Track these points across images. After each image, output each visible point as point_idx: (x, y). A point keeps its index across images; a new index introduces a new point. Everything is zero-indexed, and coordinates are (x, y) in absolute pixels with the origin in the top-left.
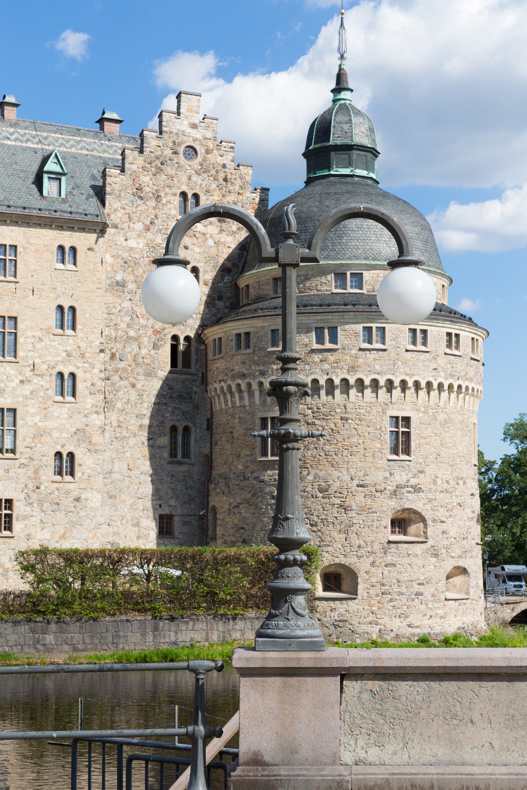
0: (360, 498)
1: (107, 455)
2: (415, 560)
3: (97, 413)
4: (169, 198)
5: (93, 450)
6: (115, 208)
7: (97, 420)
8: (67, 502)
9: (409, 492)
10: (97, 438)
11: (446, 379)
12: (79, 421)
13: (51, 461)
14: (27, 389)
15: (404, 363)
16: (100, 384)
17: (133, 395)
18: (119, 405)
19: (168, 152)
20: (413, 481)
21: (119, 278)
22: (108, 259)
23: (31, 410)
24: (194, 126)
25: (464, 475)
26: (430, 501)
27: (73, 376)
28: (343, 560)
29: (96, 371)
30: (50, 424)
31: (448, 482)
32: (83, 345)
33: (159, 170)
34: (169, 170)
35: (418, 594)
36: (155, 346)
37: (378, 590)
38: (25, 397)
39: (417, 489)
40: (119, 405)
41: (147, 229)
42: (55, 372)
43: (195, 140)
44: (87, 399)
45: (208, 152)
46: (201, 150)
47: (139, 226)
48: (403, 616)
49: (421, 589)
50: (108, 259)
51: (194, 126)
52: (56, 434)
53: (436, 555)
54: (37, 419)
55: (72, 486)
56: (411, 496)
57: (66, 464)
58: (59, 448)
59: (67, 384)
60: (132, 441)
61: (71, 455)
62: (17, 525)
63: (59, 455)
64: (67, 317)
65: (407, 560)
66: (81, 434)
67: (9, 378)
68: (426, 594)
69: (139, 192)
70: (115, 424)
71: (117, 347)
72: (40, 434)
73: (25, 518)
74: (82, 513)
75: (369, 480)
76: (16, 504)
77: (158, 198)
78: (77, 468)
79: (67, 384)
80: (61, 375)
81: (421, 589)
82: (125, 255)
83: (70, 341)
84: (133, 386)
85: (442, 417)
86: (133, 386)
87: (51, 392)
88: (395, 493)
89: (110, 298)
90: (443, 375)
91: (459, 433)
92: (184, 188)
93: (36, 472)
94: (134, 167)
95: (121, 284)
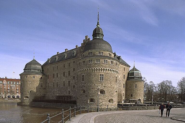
7: (77, 81)
10: (77, 83)
49: (84, 101)
57: (74, 87)
81: (84, 101)
85: (89, 74)
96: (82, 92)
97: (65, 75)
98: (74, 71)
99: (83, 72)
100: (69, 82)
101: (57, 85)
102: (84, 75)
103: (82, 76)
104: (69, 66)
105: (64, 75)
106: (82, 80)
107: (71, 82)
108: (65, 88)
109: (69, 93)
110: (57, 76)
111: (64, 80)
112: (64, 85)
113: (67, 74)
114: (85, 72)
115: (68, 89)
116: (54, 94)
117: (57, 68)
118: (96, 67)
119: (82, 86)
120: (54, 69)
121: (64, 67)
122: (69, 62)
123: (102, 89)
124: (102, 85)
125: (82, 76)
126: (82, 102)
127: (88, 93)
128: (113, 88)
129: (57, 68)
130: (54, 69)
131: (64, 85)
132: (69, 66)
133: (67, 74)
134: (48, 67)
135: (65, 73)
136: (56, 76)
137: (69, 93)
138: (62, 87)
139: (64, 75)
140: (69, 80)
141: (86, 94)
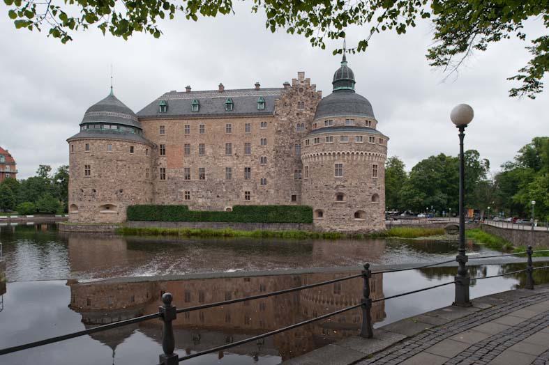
0: (325, 190)
1: (276, 179)
5: (272, 178)
7: (273, 170)
13: (260, 181)
14: (253, 162)
15: (339, 147)
16: (274, 160)
19: (294, 91)
24: (302, 82)
28: (321, 208)
33: (291, 97)
36: (290, 148)
37: (331, 217)
39: (344, 187)
46: (304, 89)
47: (285, 114)
51: (302, 82)
57: (264, 182)
62: (251, 199)
64: (264, 141)
67: (248, 160)
69: (285, 104)
71: (278, 149)
72: (257, 174)
77: (291, 105)
79: (263, 160)
80: (262, 158)
85: (355, 163)
93: (256, 184)
95: (280, 131)
97: (234, 152)
101: (202, 176)
105: (229, 151)
107: (254, 170)
109: (247, 197)
110: (202, 151)
111: (229, 162)
112: (229, 176)
113: (238, 148)
115: (242, 187)
116: (188, 197)
121: (229, 130)
122: (249, 121)
125: (334, 166)
131: (229, 176)
133: (238, 148)
135: (233, 146)
137: (247, 197)
138: (220, 181)
139: (229, 151)
140: (248, 166)
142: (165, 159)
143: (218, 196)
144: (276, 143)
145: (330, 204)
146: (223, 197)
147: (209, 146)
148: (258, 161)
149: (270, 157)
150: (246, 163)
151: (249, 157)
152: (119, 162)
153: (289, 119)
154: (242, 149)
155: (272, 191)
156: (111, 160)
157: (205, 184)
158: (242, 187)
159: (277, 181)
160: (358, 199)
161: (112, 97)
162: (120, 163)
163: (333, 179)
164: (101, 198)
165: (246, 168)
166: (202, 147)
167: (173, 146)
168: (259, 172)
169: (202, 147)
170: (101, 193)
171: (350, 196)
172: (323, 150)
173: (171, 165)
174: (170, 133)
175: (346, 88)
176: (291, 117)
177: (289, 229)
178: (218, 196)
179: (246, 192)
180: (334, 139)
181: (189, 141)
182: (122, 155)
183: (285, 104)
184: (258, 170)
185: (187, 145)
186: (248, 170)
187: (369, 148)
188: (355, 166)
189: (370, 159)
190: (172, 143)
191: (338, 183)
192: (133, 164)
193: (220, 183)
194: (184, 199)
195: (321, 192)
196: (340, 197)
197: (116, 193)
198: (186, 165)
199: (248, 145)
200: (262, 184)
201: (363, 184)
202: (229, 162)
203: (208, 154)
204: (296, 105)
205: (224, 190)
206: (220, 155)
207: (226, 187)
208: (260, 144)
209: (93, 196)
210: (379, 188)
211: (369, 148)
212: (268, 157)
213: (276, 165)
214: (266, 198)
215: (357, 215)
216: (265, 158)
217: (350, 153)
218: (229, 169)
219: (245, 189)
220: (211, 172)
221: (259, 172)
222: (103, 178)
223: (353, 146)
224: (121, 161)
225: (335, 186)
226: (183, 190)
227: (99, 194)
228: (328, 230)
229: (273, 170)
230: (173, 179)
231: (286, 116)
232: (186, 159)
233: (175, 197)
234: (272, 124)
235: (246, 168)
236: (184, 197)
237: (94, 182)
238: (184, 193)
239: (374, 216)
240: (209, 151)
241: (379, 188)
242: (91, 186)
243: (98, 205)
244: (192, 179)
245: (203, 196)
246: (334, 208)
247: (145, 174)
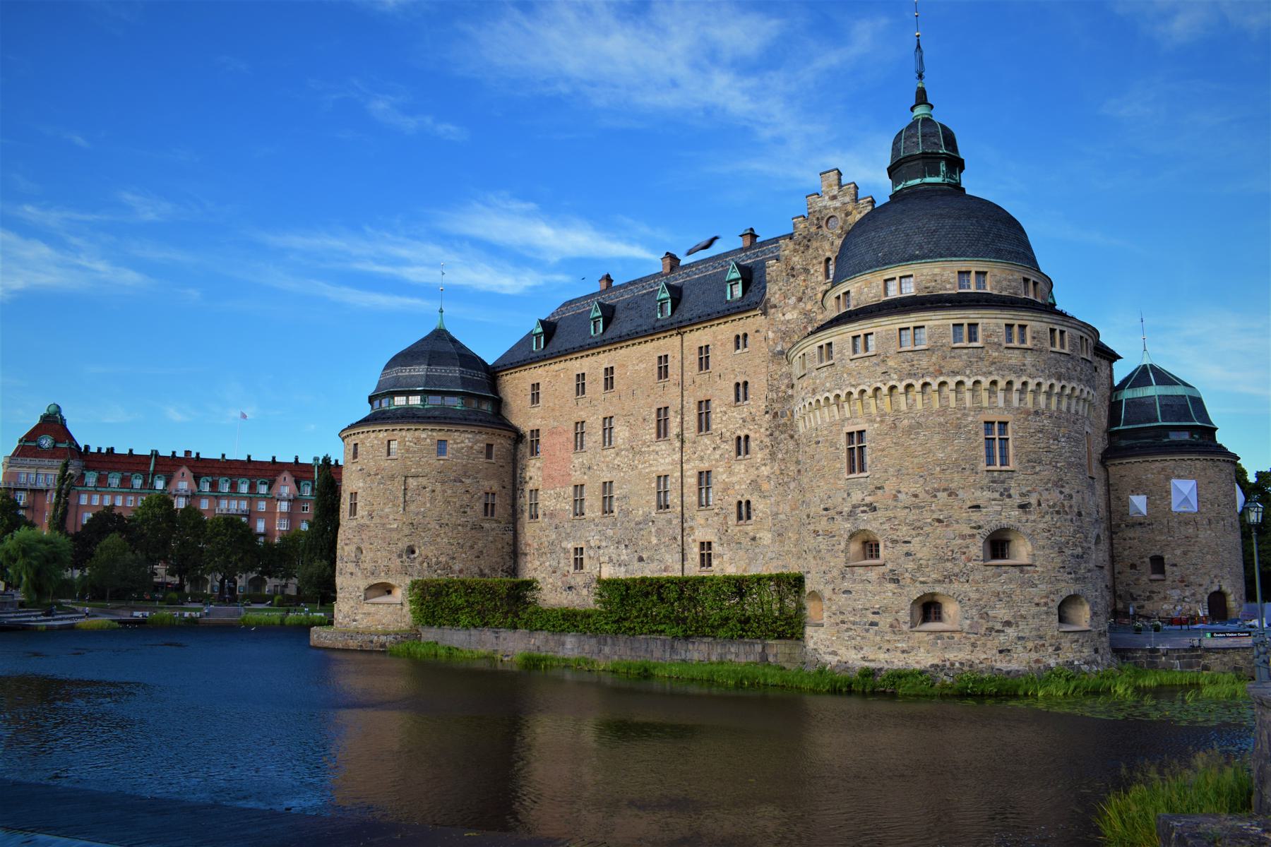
1: (773, 499)
2: (870, 587)
3: (765, 465)
4: (817, 267)
6: (774, 292)
7: (765, 471)
8: (746, 542)
9: (864, 512)
10: (765, 487)
11: (901, 380)
12: (753, 472)
13: (735, 510)
14: (718, 452)
16: (767, 441)
17: (791, 444)
18: (780, 456)
19: (813, 229)
20: (868, 500)
21: (779, 348)
22: (771, 335)
23: (721, 470)
25: (953, 486)
26: (889, 519)
27: (747, 437)
29: (762, 430)
30: (734, 479)
31: (916, 496)
32: (753, 411)
34: (814, 244)
35: (873, 624)
38: (717, 461)
40: (780, 456)
41: (800, 300)
42: (734, 437)
43: (835, 209)
44: (758, 455)
45: (848, 214)
47: (793, 300)
48: (858, 648)
49: (876, 618)
50: (771, 335)
51: (834, 198)
52: (737, 487)
53: (896, 581)
54: (724, 477)
55: (750, 528)
56: (865, 516)
57: (744, 511)
58: (739, 498)
59: (742, 445)
60: (792, 485)
61: (748, 502)
62: (715, 562)
63: (740, 503)
64: (742, 391)
65: (859, 587)
66: (755, 484)
68: (881, 624)
70: (778, 472)
71: (777, 406)
73: (721, 556)
74: (757, 550)
75: (829, 504)
76: (714, 545)
77: (806, 271)
78: (753, 513)
80: (739, 438)
81: (876, 618)
82: (783, 328)
83: (745, 409)
84: (792, 437)
86: (792, 437)
87: (733, 454)
88: (852, 514)
89: (772, 367)
90: (895, 377)
91: (936, 438)
92: (828, 254)
94: (787, 252)
96: (855, 547)
98: (737, 399)
99: (860, 412)
100: (704, 478)
102: (861, 433)
103: (850, 434)
104: (704, 363)
106: (845, 465)
107: (720, 477)
108: (670, 522)
109: (706, 560)
114: (873, 410)
116: (579, 564)
117: (609, 383)
118: (955, 373)
119: (854, 507)
120: (581, 388)
123: (1005, 523)
124: (1010, 496)
125: (843, 439)
126: (854, 623)
127: (908, 554)
128: (1079, 514)
129: (609, 383)
130: (581, 388)
132: (704, 363)
134: (555, 376)
136: (594, 437)
137: (706, 560)
138: (647, 515)
139: (662, 430)
140: (705, 466)
141: (889, 566)
142: (538, 464)
143: (641, 559)
144: (771, 388)
145: (835, 573)
146: (651, 559)
147: (622, 421)
148: (730, 447)
149: (758, 436)
150: (702, 459)
151: (706, 441)
152: (410, 480)
153: (806, 314)
154: (692, 419)
155: (766, 537)
156: (392, 478)
157: (615, 524)
158: (692, 528)
159: (778, 503)
160: (921, 549)
161: (440, 335)
162: (412, 483)
163: (841, 483)
164: (368, 565)
165: (700, 473)
166: (608, 420)
167: (552, 433)
168: (734, 478)
169: (608, 420)
170: (371, 555)
171: (894, 542)
172: (814, 392)
173: (549, 478)
174: (544, 399)
175: (918, 181)
176: (809, 307)
177: (740, 656)
178: (641, 559)
179: (702, 543)
180: (834, 348)
181: (583, 415)
182: (418, 464)
183: (792, 273)
184: (731, 474)
185: (580, 424)
186: (704, 478)
187: (957, 364)
188: (910, 430)
189: (953, 404)
190: (553, 424)
191: (857, 497)
192: (443, 483)
193: (648, 520)
194: (572, 569)
195: (816, 532)
196: (871, 548)
197: (400, 556)
198: (577, 477)
199: (704, 408)
200: (740, 517)
201: (942, 496)
202: (664, 458)
203: (620, 441)
204: (822, 269)
205: (654, 540)
206: (644, 443)
207: (659, 531)
208: (733, 398)
209: (357, 563)
210: (1023, 507)
211: (957, 364)
212: (752, 435)
213: (773, 455)
214: (751, 560)
215: (929, 609)
216: (747, 437)
217: (885, 389)
218: (662, 478)
219: (701, 535)
220: (626, 489)
221: (734, 478)
222: (377, 520)
223: (891, 363)
224: (415, 476)
225: (846, 509)
226: (570, 546)
227: (367, 556)
228: (833, 660)
229: (765, 471)
230: (552, 515)
231: (794, 308)
232: (578, 460)
233: (555, 563)
234: (760, 337)
235: (700, 473)
236: (572, 562)
237: (362, 527)
238: (572, 551)
239: (1002, 613)
240: (621, 433)
241: (1023, 507)
242: (355, 540)
243: (363, 584)
244: (588, 514)
245: (611, 560)
246: (846, 585)
247: (479, 507)
